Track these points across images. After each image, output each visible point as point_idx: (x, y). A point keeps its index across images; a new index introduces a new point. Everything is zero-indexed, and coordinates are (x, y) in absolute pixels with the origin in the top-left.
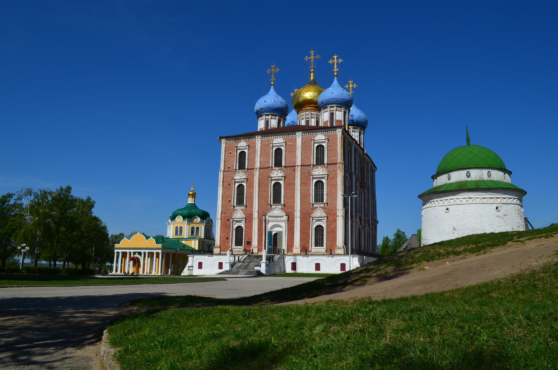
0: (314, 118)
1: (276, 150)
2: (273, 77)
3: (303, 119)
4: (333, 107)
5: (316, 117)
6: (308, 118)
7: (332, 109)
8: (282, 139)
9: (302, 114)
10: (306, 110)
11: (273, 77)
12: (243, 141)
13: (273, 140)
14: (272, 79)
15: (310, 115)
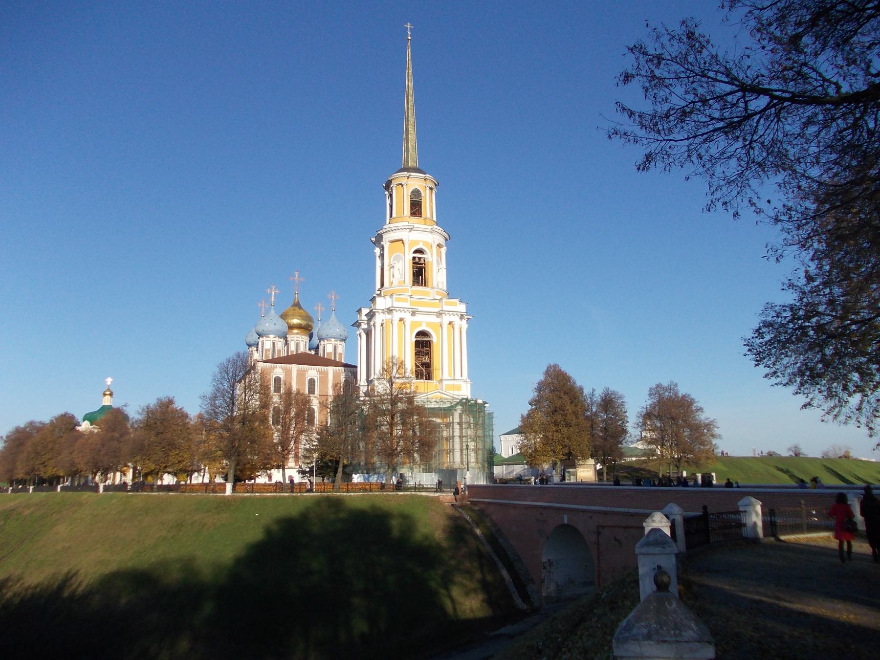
0: (303, 341)
1: (309, 380)
2: (273, 298)
3: (293, 340)
4: (336, 341)
5: (304, 341)
6: (299, 341)
7: (336, 343)
8: (316, 371)
9: (292, 336)
10: (297, 334)
11: (273, 298)
12: (278, 367)
13: (308, 371)
14: (272, 299)
15: (300, 338)
